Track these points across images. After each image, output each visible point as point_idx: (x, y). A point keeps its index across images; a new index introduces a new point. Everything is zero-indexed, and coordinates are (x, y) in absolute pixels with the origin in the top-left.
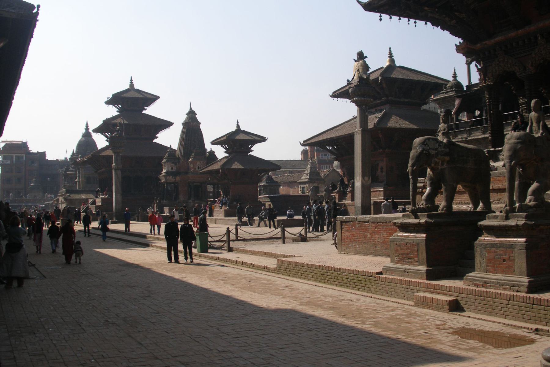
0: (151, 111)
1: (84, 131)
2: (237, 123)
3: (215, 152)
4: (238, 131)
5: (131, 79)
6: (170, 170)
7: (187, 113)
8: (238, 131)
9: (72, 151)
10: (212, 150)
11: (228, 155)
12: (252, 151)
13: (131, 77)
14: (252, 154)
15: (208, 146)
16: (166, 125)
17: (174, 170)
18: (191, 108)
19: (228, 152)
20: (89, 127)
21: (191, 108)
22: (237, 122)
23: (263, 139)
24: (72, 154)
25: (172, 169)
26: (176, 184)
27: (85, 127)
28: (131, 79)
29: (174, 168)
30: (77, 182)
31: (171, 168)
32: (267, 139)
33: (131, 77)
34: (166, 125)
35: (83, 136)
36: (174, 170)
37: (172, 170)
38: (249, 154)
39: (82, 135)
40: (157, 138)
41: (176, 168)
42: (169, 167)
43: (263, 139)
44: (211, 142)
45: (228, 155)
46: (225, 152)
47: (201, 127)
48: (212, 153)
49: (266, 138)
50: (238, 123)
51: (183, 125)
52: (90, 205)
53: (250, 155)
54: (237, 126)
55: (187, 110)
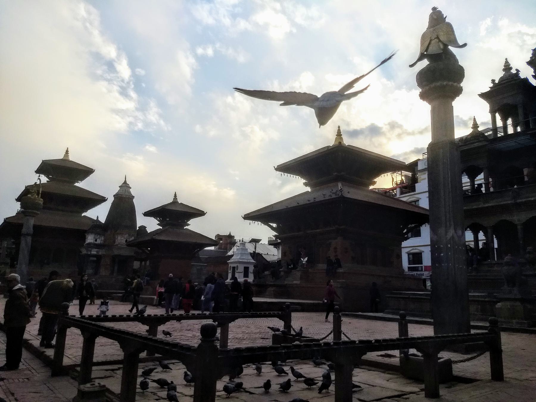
4: (175, 202)
8: (175, 202)
11: (161, 228)
12: (188, 225)
15: (141, 221)
16: (99, 200)
18: (125, 181)
21: (125, 181)
23: (200, 213)
31: (95, 239)
34: (99, 200)
37: (96, 242)
38: (185, 228)
43: (200, 213)
45: (161, 228)
46: (158, 224)
47: (134, 200)
48: (143, 228)
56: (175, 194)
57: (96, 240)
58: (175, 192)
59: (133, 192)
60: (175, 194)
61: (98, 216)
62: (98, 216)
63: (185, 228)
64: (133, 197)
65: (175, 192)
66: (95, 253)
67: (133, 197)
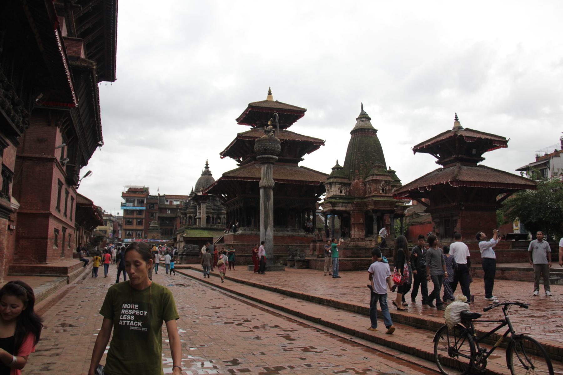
0: (297, 128)
1: (204, 169)
2: (455, 118)
3: (395, 172)
5: (270, 90)
6: (338, 193)
7: (357, 117)
8: (458, 128)
9: (191, 189)
10: (392, 169)
11: (442, 167)
12: (483, 159)
13: (270, 88)
14: (483, 164)
17: (344, 195)
18: (362, 110)
19: (443, 161)
20: (209, 166)
21: (362, 110)
22: (455, 116)
23: (501, 142)
24: (191, 192)
25: (341, 192)
26: (345, 215)
27: (205, 166)
28: (270, 90)
29: (343, 191)
30: (197, 219)
31: (339, 191)
32: (509, 140)
33: (270, 88)
35: (202, 175)
36: (343, 194)
37: (341, 194)
38: (478, 164)
39: (202, 173)
40: (302, 160)
41: (347, 192)
42: (337, 190)
44: (413, 148)
45: (442, 167)
46: (438, 163)
49: (507, 139)
50: (456, 117)
51: (351, 135)
52: (218, 243)
53: (480, 166)
54: (455, 122)
55: (358, 114)
56: (456, 115)
57: (341, 192)
58: (456, 114)
59: (374, 123)
60: (456, 115)
61: (337, 161)
62: (337, 161)
63: (478, 164)
64: (376, 131)
65: (456, 114)
66: (343, 209)
67: (376, 131)
